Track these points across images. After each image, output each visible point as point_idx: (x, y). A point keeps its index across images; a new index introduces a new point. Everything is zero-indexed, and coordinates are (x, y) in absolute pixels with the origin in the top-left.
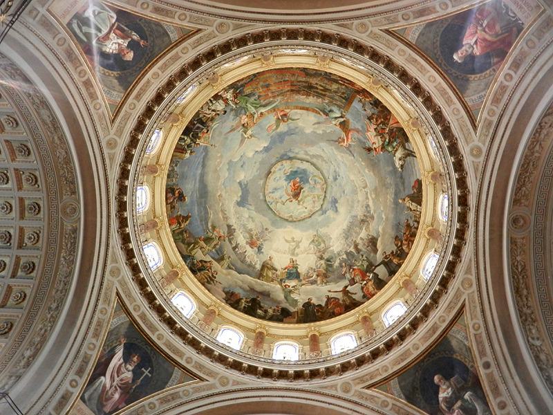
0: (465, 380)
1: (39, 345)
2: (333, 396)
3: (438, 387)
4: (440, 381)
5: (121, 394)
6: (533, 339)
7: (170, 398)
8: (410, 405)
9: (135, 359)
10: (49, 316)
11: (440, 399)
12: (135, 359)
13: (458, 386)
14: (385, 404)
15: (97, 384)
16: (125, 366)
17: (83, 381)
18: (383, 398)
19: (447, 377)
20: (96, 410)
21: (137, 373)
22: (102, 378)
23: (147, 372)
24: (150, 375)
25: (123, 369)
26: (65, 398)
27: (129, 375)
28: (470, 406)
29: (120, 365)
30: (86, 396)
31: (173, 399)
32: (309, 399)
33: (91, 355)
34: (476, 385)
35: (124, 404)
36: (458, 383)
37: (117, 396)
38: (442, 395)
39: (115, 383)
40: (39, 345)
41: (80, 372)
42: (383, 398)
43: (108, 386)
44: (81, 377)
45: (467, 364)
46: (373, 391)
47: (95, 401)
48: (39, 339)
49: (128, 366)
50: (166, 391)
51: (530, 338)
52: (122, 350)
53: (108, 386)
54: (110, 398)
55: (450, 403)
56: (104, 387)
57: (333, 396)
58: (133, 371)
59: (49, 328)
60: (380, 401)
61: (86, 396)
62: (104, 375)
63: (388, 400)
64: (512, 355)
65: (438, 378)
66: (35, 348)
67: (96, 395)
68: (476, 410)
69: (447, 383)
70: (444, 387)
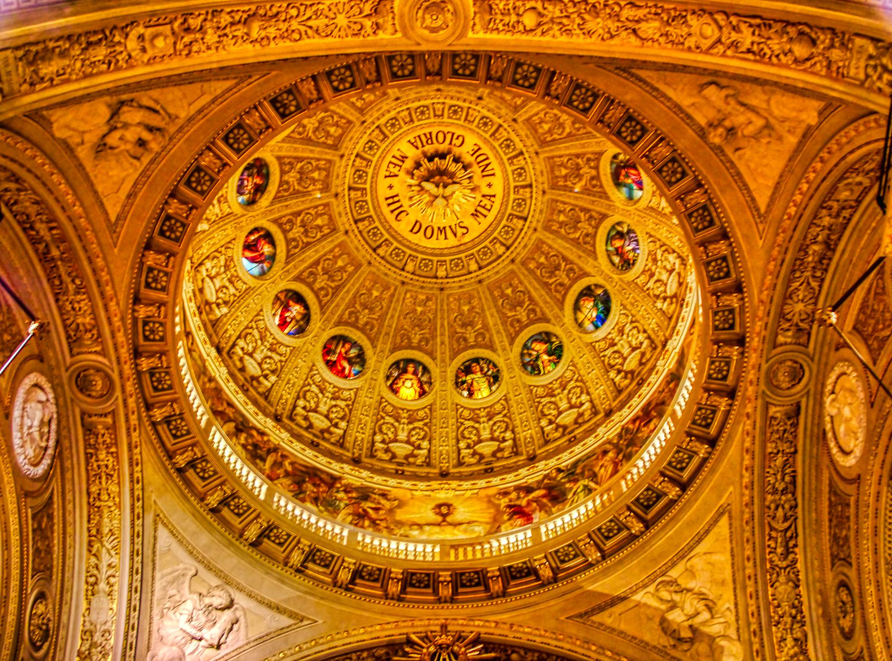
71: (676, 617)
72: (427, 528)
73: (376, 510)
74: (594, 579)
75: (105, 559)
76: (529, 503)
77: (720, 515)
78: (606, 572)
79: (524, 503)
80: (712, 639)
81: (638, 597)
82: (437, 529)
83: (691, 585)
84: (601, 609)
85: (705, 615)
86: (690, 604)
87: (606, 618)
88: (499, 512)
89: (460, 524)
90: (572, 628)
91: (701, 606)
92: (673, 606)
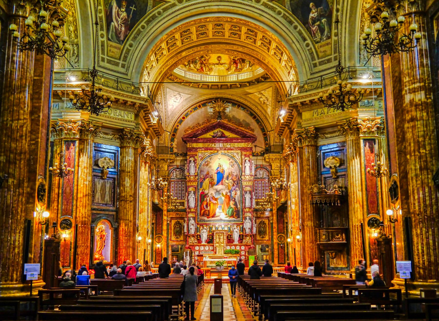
0: (326, 11)
1: (75, 23)
2: (250, 6)
3: (310, 10)
4: (313, 7)
5: (125, 27)
6: (366, 3)
7: (151, 19)
8: (294, 15)
9: (124, 4)
10: (69, 3)
11: (310, 17)
12: (124, 4)
13: (321, 13)
14: (279, 13)
15: (111, 28)
16: (120, 10)
17: (104, 33)
18: (279, 9)
19: (317, 6)
20: (117, 41)
21: (128, 11)
22: (112, 23)
23: (133, 8)
24: (135, 9)
25: (120, 13)
26: (103, 45)
27: (124, 15)
28: (323, 27)
29: (118, 11)
30: (110, 37)
31: (153, 19)
32: (235, 7)
33: (102, 16)
34: (330, 17)
35: (128, 31)
36: (322, 12)
37: (123, 29)
38: (311, 15)
39: (119, 23)
40: (75, 23)
41: (102, 29)
42: (279, 9)
43: (117, 26)
44: (103, 30)
45: (329, 3)
46: (273, 4)
47: (114, 37)
48: (72, 19)
49: (122, 9)
50: (148, 15)
51: (364, 3)
52: (115, 2)
53: (117, 26)
54: (121, 32)
55: (314, 21)
56: (115, 27)
57: (250, 6)
58: (126, 11)
59: (74, 11)
60: (277, 11)
61: (110, 37)
62: (113, 21)
63: (282, 11)
64: (351, 11)
65: (312, 5)
66: (74, 25)
67: (114, 34)
68: (325, 30)
69: (316, 9)
70: (314, 11)
71: (261, 99)
72: (216, 65)
73: (205, 60)
74: (248, 89)
75: (159, 98)
76: (238, 59)
77: (271, 87)
78: (250, 89)
79: (236, 59)
80: (267, 105)
81: (255, 94)
82: (218, 66)
83: (265, 95)
84: (248, 94)
85: (266, 101)
86: (264, 98)
87: (250, 96)
88: (231, 61)
89: (223, 64)
90: (243, 97)
91: (266, 99)
92: (261, 97)
